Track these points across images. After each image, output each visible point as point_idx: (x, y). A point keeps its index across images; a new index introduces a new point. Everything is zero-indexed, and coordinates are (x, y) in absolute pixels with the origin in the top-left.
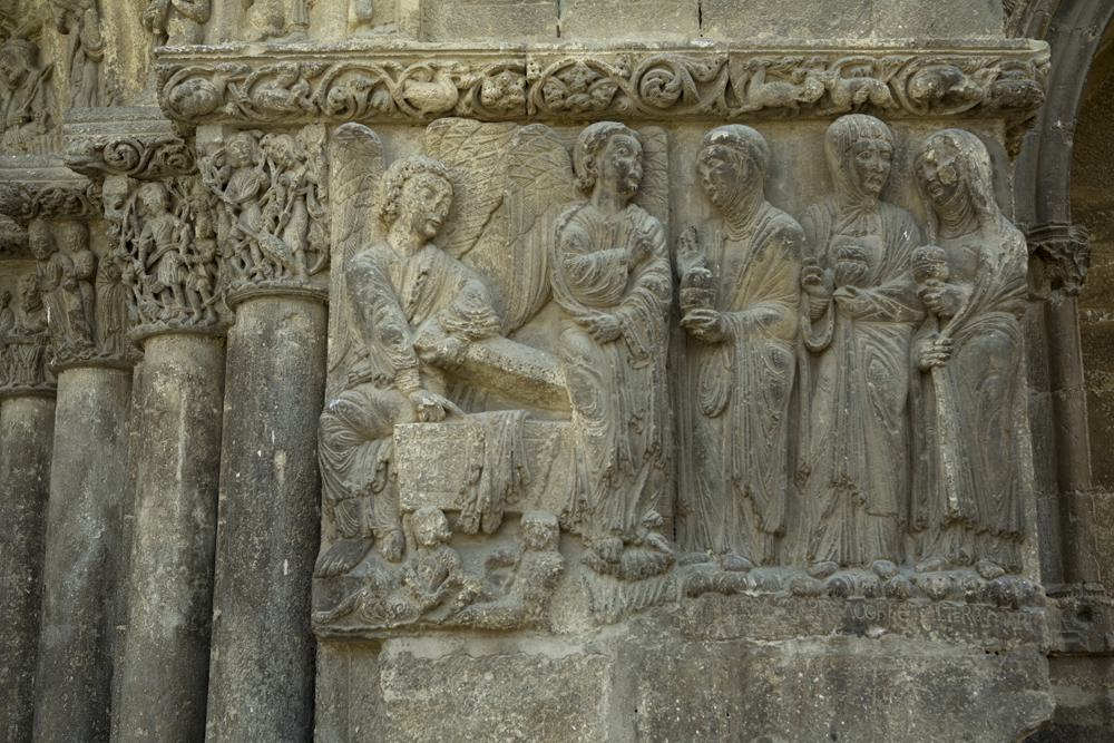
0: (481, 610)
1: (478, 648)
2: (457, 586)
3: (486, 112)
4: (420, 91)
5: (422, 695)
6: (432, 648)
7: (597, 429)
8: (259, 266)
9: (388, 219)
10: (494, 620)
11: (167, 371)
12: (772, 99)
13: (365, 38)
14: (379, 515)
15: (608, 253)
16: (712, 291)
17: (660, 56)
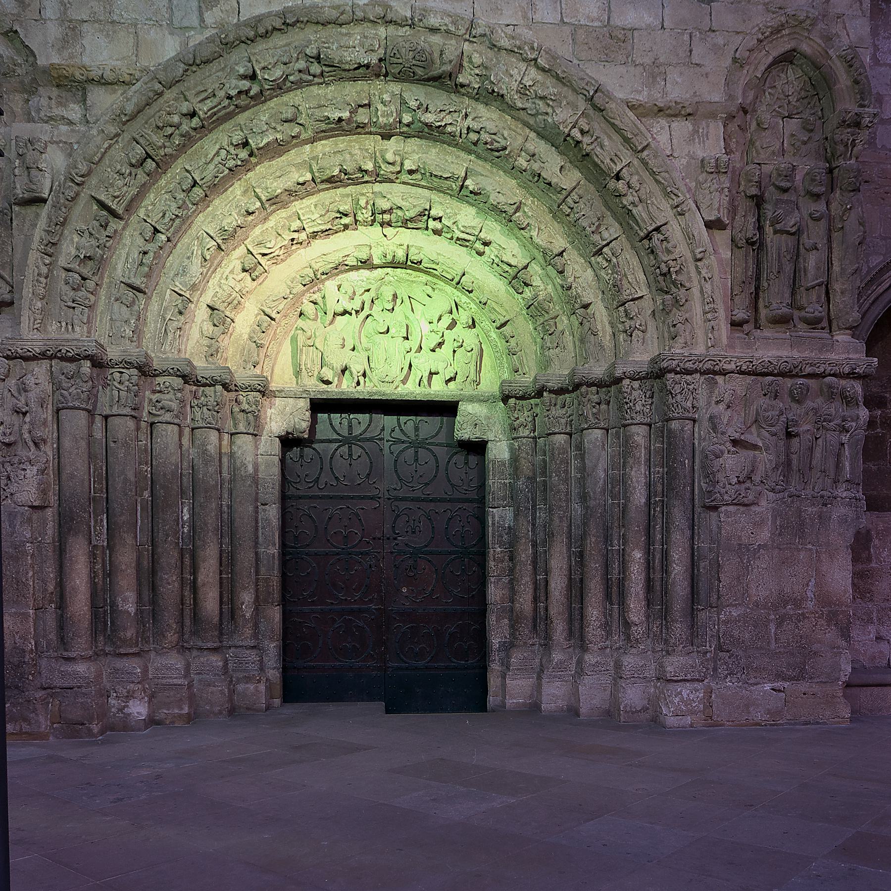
0: (746, 501)
1: (742, 509)
2: (740, 494)
3: (741, 372)
4: (726, 367)
5: (729, 519)
6: (732, 508)
7: (771, 457)
8: (681, 411)
9: (717, 402)
10: (748, 503)
11: (638, 434)
12: (811, 372)
13: (712, 351)
14: (720, 476)
15: (773, 413)
16: (796, 423)
17: (786, 360)
